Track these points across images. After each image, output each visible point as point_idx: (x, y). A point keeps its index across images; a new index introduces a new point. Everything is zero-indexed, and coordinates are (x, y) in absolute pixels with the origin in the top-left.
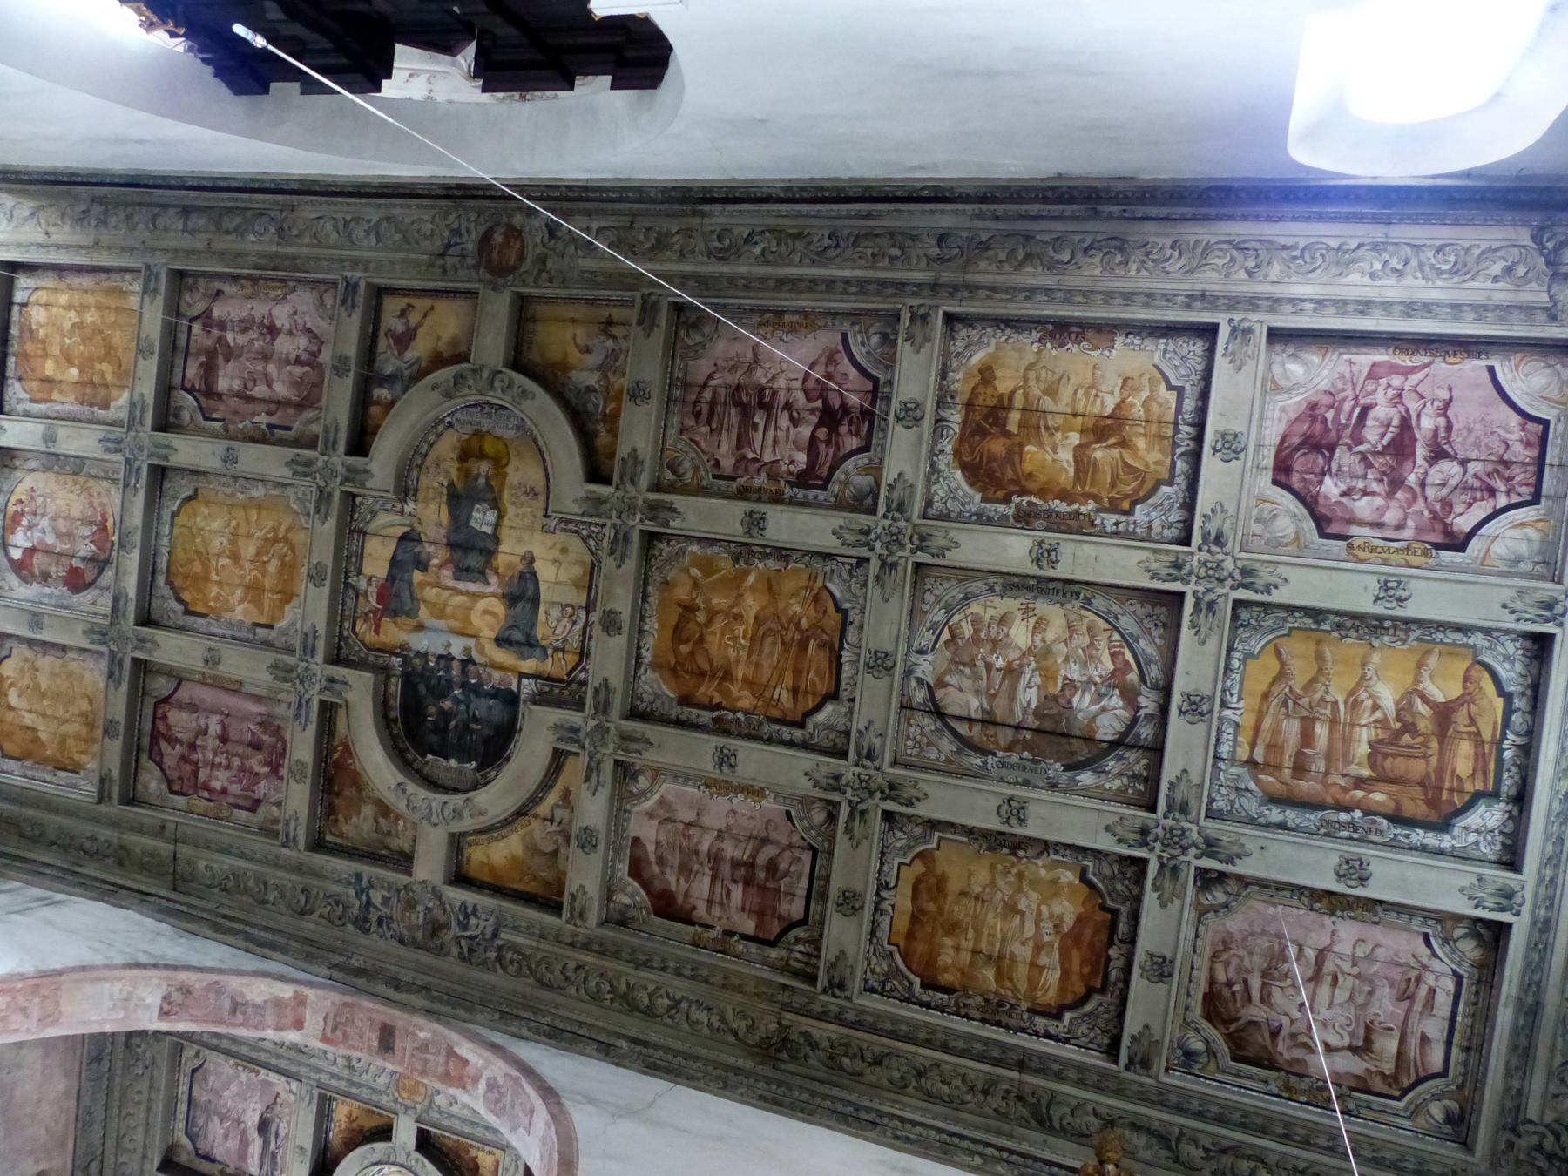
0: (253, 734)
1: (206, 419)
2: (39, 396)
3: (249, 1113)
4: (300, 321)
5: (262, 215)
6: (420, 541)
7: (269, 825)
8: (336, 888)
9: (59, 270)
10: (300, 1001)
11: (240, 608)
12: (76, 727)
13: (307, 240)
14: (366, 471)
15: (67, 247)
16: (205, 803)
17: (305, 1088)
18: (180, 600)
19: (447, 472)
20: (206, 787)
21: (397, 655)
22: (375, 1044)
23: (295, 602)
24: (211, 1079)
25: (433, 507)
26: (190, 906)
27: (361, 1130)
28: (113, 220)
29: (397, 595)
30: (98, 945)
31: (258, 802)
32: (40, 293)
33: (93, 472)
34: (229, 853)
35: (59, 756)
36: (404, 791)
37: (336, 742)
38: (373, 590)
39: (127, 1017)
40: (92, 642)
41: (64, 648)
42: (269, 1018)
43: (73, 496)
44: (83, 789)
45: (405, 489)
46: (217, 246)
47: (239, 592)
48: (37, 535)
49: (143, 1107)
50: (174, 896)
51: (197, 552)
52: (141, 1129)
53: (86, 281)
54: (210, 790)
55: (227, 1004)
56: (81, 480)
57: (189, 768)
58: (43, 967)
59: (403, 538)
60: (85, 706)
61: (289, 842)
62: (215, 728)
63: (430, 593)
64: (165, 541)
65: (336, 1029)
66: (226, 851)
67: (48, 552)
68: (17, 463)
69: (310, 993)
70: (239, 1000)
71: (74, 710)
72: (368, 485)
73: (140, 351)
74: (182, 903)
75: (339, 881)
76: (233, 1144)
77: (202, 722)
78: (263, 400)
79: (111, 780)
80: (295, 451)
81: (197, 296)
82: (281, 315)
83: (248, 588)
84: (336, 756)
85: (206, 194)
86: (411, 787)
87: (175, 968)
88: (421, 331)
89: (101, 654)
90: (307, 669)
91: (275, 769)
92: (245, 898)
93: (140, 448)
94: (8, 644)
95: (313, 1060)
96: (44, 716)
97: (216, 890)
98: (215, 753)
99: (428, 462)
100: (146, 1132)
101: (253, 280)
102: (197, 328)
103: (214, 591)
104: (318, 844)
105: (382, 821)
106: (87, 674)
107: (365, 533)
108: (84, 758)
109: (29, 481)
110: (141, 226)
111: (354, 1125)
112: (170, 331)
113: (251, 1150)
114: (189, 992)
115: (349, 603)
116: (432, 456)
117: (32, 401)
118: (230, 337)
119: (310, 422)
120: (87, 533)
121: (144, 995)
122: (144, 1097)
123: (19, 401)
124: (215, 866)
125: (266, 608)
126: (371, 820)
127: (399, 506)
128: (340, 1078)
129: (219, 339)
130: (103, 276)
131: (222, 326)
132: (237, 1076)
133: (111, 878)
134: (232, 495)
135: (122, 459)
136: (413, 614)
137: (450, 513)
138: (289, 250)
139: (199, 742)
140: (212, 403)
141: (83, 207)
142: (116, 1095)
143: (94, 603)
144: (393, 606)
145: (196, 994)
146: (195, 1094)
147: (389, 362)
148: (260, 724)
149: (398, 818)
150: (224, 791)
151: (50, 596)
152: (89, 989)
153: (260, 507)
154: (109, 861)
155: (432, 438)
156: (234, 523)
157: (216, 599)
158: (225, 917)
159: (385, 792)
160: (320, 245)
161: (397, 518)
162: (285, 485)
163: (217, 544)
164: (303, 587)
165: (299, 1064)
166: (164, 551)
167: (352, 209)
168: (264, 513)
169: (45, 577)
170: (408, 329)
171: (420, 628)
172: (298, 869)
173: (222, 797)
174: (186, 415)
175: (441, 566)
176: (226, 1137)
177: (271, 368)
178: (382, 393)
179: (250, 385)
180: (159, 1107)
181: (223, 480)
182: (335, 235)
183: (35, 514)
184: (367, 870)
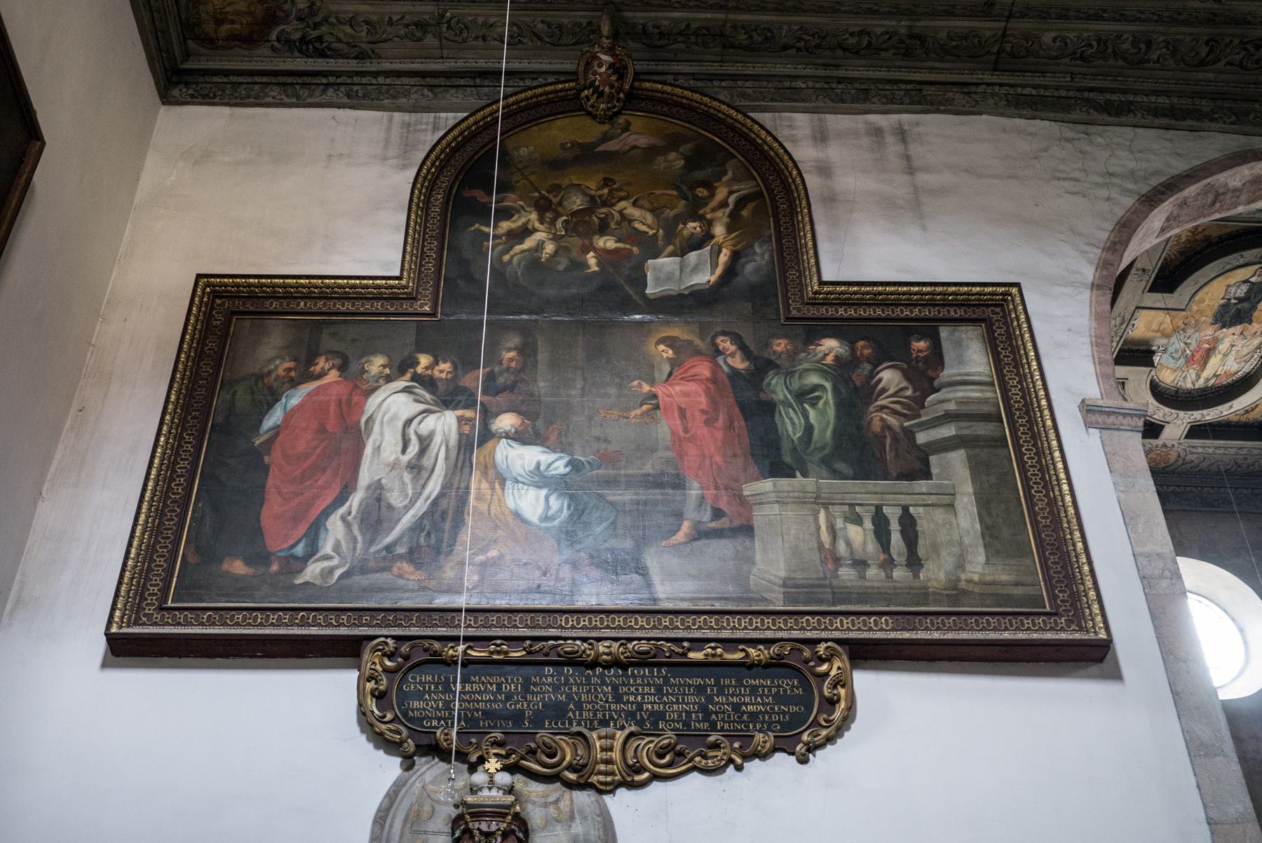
26: (1035, 87)
92: (1111, 62)
111: (1198, 237)
124: (1071, 35)
133: (911, 77)
158: (1091, 90)
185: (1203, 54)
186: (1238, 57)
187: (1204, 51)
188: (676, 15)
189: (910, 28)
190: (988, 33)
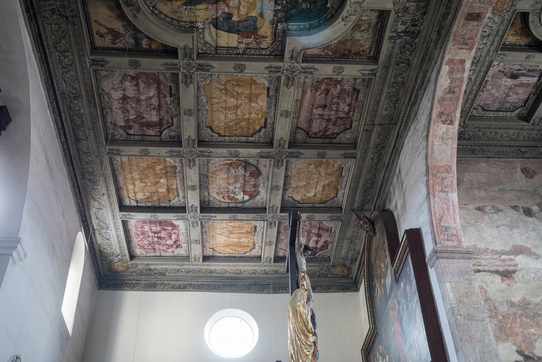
0: (321, 93)
1: (173, 125)
2: (175, 193)
3: (507, 84)
4: (117, 86)
5: (70, 107)
6: (217, 18)
7: (365, 84)
8: (397, 49)
9: (118, 190)
10: (451, 61)
11: (261, 104)
12: (322, 170)
13: (77, 85)
14: (185, 48)
15: (107, 187)
16: (355, 113)
17: (497, 58)
18: (260, 130)
19: (179, 7)
20: (348, 113)
21: (277, 26)
22: (475, 23)
23: (255, 78)
24: (488, 102)
25: (198, 13)
26: (404, 117)
27: (522, 29)
28: (90, 170)
29: (246, 28)
30: (418, 153)
31: (354, 89)
32: (130, 196)
33: (206, 170)
34: (379, 100)
35: (335, 175)
36: (346, 17)
37: (323, 53)
38: (245, 41)
39: (451, 139)
40: (283, 165)
41: (286, 177)
42: (459, 76)
43: (218, 177)
44: (350, 164)
45: (192, 28)
46: (90, 126)
47: (253, 105)
48: (237, 190)
49: (498, 131)
50: (399, 124)
51: (236, 124)
52: (509, 131)
53: (121, 179)
54: (349, 111)
55: (449, 96)
56: (210, 174)
57: (339, 121)
58: (425, 174)
59: (216, 27)
60: (312, 166)
61: (373, 73)
62: (319, 111)
63: (243, 11)
64: (233, 139)
65: (466, 44)
66: (378, 102)
67: (244, 185)
68: (207, 200)
69: (447, 57)
70: (448, 90)
71: (314, 171)
72: (191, 47)
73: (146, 155)
74: (403, 120)
75: (393, 47)
76: (521, 90)
77: (316, 117)
78: (159, 100)
79: (345, 154)
80: (180, 83)
81: (116, 133)
82: (117, 95)
83: (250, 101)
84: (330, 53)
85: (67, 132)
86: (344, 14)
87: (430, 119)
88: (109, 26)
89: (287, 161)
90: (287, 70)
91: (338, 82)
92: (401, 92)
93: (191, 151)
94: (287, 198)
95: (483, 55)
96: (318, 182)
97: (397, 105)
98: (332, 110)
99: (176, 17)
100: (510, 129)
101: (102, 109)
102: (131, 132)
103: (253, 115)
104: (375, 59)
105: (363, 28)
106: (297, 167)
107: (217, 47)
108: (336, 165)
109: (214, 195)
110: (90, 158)
111: (519, 32)
112: (135, 143)
113: (525, 82)
114: (442, 113)
115: (252, 52)
116: (172, 16)
117: (178, 196)
118: (132, 117)
119: (165, 78)
120: (234, 171)
121: (441, 132)
122: (494, 130)
123: (179, 200)
124: (385, 106)
125: (260, 91)
126: (363, 33)
127: (200, 30)
128: (494, 41)
129: (134, 122)
130: (117, 172)
131: (128, 121)
132: (488, 90)
133: (390, 151)
134: (207, 110)
135: (197, 158)
136: (255, 20)
137: (200, 4)
138: (83, 93)
139: (327, 118)
140: (165, 122)
141: (88, 182)
142: (491, 142)
143: (265, 166)
144: (252, 30)
145: (443, 109)
146: (495, 109)
147: (128, 41)
148: (316, 91)
149: (361, 20)
150: (350, 105)
151: (264, 183)
152: (436, 155)
153: (211, 98)
154: (383, 152)
155: (163, 16)
156: (220, 109)
157: (258, 114)
158: (409, 100)
159: (347, 27)
160: (77, 79)
161: (207, 31)
162: (198, 87)
163: (231, 116)
164: (247, 74)
165: (484, 61)
166: (237, 139)
167: (55, 64)
168: (213, 96)
169: (255, 186)
170: (109, 33)
171: (261, 15)
172: (387, 67)
173: (353, 106)
174: (172, 134)
175: (228, 6)
176: (517, 94)
177: (143, 97)
178: (144, 43)
179: (153, 106)
180: (499, 124)
181: (200, 115)
182: (70, 72)
183: (228, 192)
184: (388, 34)
185: (404, 65)
186: (408, 53)
187: (402, 65)
188: (357, 198)
189: (372, 149)
190: (379, 129)
